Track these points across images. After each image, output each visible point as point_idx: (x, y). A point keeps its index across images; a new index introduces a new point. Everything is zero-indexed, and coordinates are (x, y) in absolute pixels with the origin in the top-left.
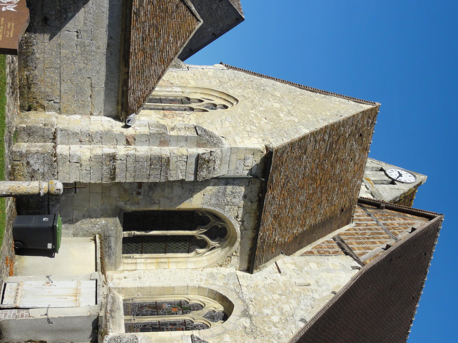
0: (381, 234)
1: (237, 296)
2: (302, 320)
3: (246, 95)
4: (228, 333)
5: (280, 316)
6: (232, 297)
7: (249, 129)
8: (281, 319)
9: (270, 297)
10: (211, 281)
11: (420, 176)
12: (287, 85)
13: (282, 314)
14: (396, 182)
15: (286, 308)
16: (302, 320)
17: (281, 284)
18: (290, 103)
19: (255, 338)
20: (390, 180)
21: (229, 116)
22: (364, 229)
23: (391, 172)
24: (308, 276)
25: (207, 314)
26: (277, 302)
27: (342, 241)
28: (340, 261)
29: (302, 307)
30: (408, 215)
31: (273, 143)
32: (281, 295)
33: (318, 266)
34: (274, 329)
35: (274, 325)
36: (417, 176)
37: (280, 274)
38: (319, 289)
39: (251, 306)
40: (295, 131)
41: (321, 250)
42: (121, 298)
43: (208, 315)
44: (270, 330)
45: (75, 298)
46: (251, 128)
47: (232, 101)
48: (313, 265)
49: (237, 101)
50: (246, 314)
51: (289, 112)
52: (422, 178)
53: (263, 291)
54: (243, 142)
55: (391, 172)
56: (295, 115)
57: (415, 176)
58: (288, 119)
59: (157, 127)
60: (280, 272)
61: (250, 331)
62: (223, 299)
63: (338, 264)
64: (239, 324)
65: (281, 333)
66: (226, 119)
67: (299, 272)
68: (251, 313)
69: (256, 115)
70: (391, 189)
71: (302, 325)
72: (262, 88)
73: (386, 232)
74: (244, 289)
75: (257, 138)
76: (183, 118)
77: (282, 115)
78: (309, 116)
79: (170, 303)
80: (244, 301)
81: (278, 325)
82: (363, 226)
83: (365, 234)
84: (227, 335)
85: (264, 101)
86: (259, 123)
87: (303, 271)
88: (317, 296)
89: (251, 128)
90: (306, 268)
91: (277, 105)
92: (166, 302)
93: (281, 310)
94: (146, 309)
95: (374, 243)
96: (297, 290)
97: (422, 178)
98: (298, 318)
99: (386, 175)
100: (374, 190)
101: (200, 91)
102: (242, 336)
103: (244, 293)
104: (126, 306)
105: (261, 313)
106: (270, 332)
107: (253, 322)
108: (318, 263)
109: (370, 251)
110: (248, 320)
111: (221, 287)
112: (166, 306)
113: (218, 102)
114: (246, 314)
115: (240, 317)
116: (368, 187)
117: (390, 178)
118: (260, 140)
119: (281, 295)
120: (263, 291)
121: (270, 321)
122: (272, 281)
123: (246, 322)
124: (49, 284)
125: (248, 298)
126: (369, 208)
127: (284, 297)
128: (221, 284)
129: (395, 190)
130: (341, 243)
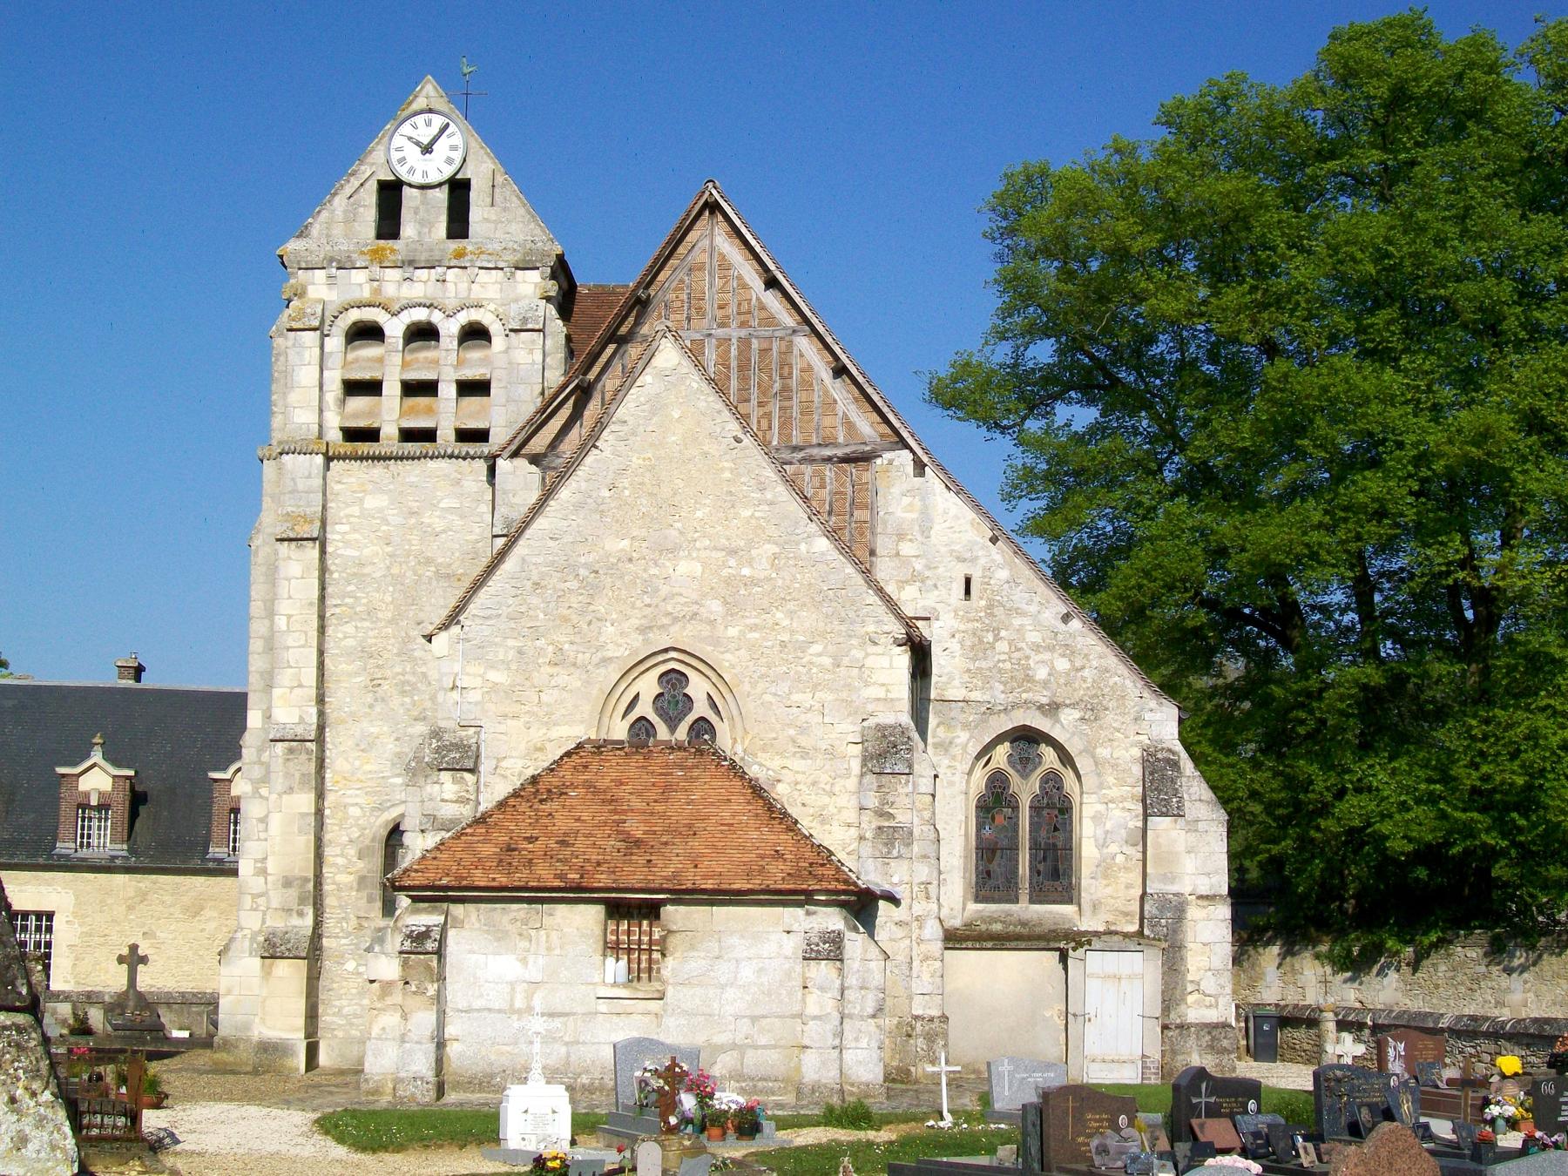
0: (764, 352)
1: (1002, 715)
2: (1066, 618)
3: (635, 622)
4: (1095, 748)
5: (1056, 655)
6: (1006, 724)
7: (827, 661)
8: (1064, 656)
9: (1003, 657)
10: (957, 751)
11: (424, 93)
12: (552, 503)
13: (1051, 649)
14: (459, 176)
15: (1034, 637)
16: (1066, 618)
17: (962, 627)
18: (675, 533)
19: (1107, 709)
20: (446, 188)
21: (761, 686)
22: (743, 378)
23: (406, 167)
24: (941, 570)
25: (1013, 767)
26: (1018, 650)
27: (796, 449)
28: (895, 491)
29: (1033, 609)
30: (681, 250)
31: (887, 628)
32: (997, 638)
33: (910, 540)
34: (1086, 673)
35: (1078, 670)
36: (420, 103)
37: (932, 621)
38: (982, 561)
39: (1024, 696)
40: (820, 567)
41: (830, 505)
42: (973, 907)
43: (1019, 767)
44: (1090, 680)
45: (1123, 982)
46: (820, 655)
47: (660, 658)
48: (907, 549)
49: (666, 650)
50: (1052, 709)
51: (733, 552)
52: (429, 92)
53: (984, 664)
54: (883, 685)
55: (406, 167)
56: (742, 543)
57: (430, 111)
58: (765, 564)
59: (890, 843)
60: (928, 619)
61: (1090, 713)
62: (999, 740)
63: (906, 500)
64: (1076, 727)
65: (1095, 663)
66: (775, 694)
67: (929, 582)
68: (1045, 701)
69: (754, 628)
70: (492, 205)
71: (1076, 624)
72: (583, 572)
73: (757, 337)
74: (976, 695)
75: (867, 655)
76: (779, 781)
77: (746, 571)
78: (747, 513)
79: (980, 827)
80: (1015, 706)
81: (1078, 664)
82: (729, 378)
83: (764, 391)
84: (1099, 751)
85: (665, 590)
86: (792, 632)
87: (927, 573)
88: (1003, 574)
89: (820, 655)
90: (918, 567)
91: (686, 567)
92: (978, 830)
93: (1037, 648)
94: (994, 867)
95: (807, 385)
96: (983, 603)
97: (429, 92)
98: (1061, 627)
99: (423, 187)
100: (513, 258)
101: (606, 720)
102: (1101, 727)
103: (986, 697)
104: (978, 899)
105: (1045, 684)
106: (1094, 681)
107: (1068, 702)
108: (901, 536)
109: (840, 408)
110: (1067, 710)
111: (971, 737)
112: (987, 832)
113: (648, 686)
114: (1052, 709)
115: (1058, 721)
116: (490, 265)
117: (440, 185)
118: (871, 649)
119: (997, 638)
120: (984, 664)
121: (1067, 674)
122: (956, 640)
123: (1069, 716)
124: (1092, 1015)
125: (1003, 696)
126: (637, 323)
127: (1003, 633)
128: (963, 736)
129: (496, 196)
130: (802, 454)
